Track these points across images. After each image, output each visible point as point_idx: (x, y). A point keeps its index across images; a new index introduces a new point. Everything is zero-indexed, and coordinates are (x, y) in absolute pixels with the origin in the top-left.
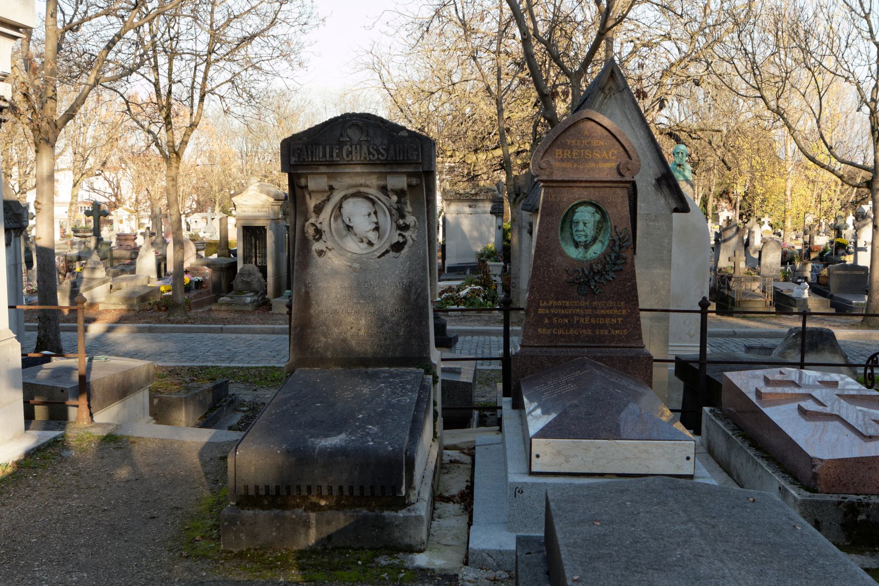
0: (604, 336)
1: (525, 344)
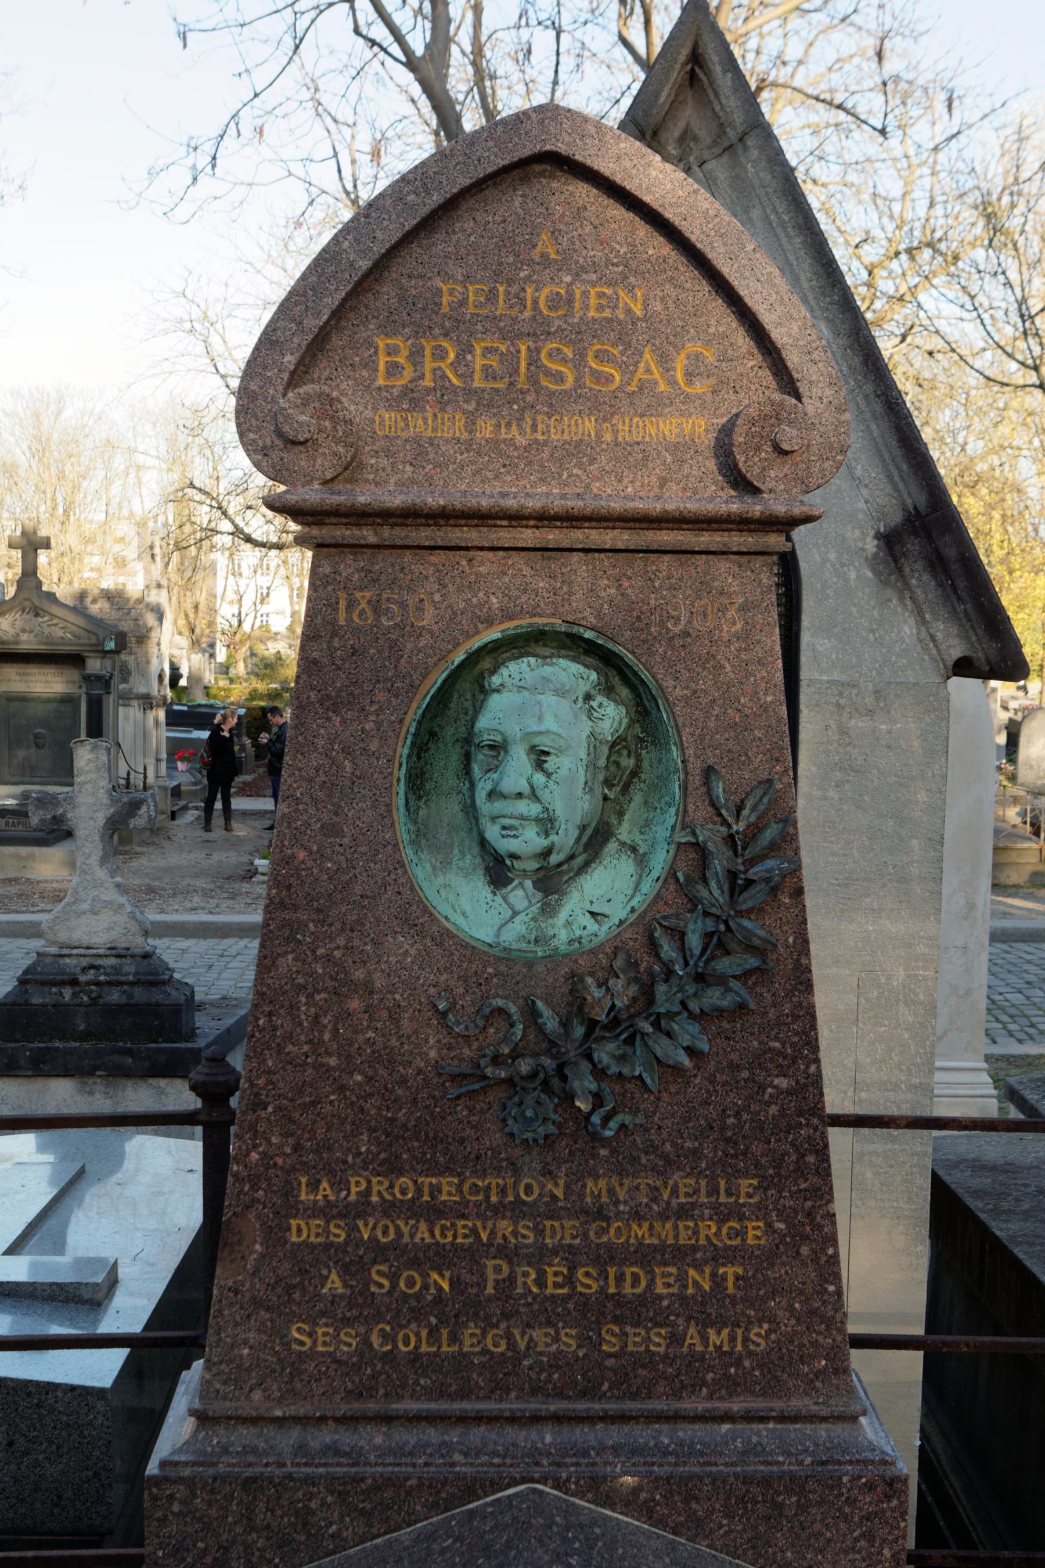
0: (648, 1360)
1: (217, 1407)
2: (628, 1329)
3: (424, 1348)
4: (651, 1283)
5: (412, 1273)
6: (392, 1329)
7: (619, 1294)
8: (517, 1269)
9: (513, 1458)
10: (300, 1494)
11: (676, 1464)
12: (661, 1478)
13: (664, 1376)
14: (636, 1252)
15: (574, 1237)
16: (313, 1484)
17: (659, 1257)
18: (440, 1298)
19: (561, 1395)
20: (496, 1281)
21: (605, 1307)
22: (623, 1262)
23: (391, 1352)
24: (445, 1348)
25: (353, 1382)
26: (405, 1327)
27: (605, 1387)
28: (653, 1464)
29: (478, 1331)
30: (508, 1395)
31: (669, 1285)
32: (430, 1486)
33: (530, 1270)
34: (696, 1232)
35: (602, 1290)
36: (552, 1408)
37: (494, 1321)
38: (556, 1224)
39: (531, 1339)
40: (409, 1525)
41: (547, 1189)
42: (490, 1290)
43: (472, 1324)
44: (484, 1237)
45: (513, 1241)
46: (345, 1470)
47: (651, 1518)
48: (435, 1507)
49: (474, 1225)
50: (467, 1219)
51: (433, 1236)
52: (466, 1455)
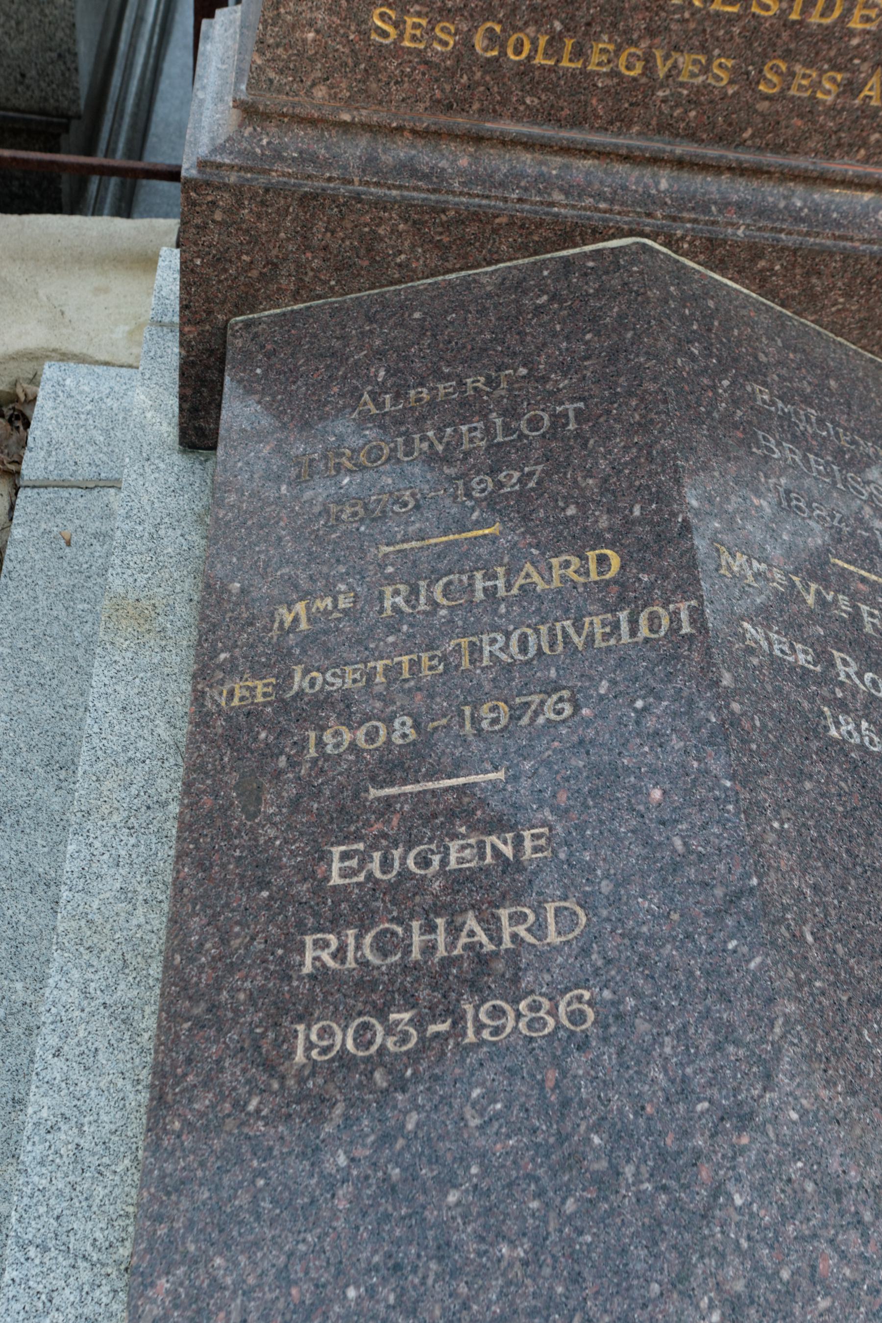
1: (269, 101)
3: (539, 60)
6: (503, 30)
7: (800, 22)
11: (808, 234)
16: (385, 209)
19: (692, 136)
23: (496, 59)
24: (565, 63)
25: (443, 91)
26: (520, 30)
28: (781, 231)
29: (611, 47)
30: (629, 128)
32: (522, 226)
36: (678, 151)
37: (635, 36)
39: (675, 66)
40: (489, 264)
43: (605, 37)
46: (423, 195)
48: (524, 250)
52: (567, 194)
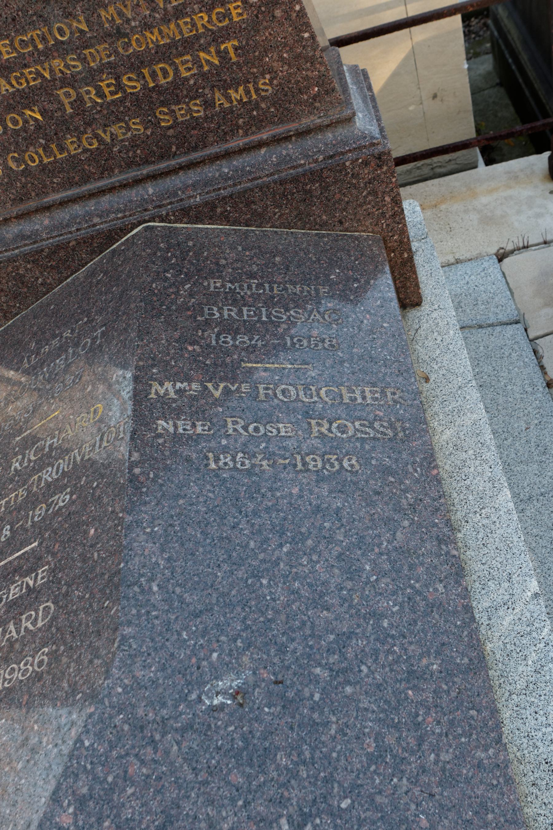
0: (195, 124)
2: (173, 107)
3: (46, 161)
4: (176, 71)
5: (12, 115)
6: (19, 155)
7: (157, 86)
8: (81, 91)
9: (131, 210)
10: (10, 269)
11: (235, 185)
12: (226, 197)
13: (210, 130)
14: (157, 53)
15: (109, 56)
16: (15, 261)
17: (174, 51)
18: (38, 126)
19: (147, 162)
20: (71, 103)
21: (151, 97)
22: (151, 63)
23: (26, 169)
24: (59, 156)
25: (13, 194)
26: (27, 151)
27: (174, 149)
28: (219, 189)
29: (75, 139)
30: (113, 172)
31: (189, 69)
32: (85, 242)
33: (89, 88)
34: (194, 25)
35: (145, 86)
36: (145, 172)
37: (82, 129)
38: (92, 51)
39: (112, 134)
40: (83, 267)
41: (74, 28)
42: (69, 110)
43: (69, 136)
44: (47, 75)
45: (69, 72)
46: (30, 247)
47: (228, 221)
48: (94, 253)
49: (37, 69)
50: (29, 67)
51: (13, 86)
52: (100, 217)
